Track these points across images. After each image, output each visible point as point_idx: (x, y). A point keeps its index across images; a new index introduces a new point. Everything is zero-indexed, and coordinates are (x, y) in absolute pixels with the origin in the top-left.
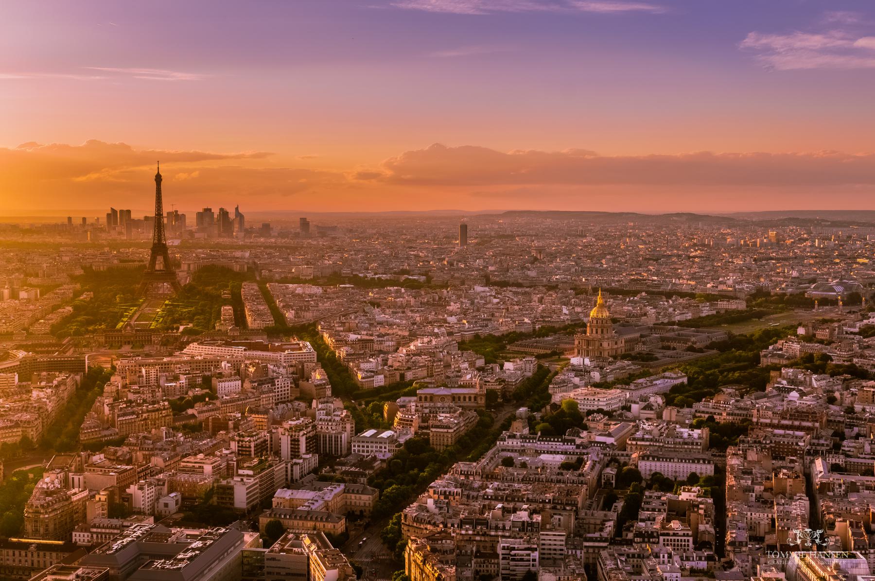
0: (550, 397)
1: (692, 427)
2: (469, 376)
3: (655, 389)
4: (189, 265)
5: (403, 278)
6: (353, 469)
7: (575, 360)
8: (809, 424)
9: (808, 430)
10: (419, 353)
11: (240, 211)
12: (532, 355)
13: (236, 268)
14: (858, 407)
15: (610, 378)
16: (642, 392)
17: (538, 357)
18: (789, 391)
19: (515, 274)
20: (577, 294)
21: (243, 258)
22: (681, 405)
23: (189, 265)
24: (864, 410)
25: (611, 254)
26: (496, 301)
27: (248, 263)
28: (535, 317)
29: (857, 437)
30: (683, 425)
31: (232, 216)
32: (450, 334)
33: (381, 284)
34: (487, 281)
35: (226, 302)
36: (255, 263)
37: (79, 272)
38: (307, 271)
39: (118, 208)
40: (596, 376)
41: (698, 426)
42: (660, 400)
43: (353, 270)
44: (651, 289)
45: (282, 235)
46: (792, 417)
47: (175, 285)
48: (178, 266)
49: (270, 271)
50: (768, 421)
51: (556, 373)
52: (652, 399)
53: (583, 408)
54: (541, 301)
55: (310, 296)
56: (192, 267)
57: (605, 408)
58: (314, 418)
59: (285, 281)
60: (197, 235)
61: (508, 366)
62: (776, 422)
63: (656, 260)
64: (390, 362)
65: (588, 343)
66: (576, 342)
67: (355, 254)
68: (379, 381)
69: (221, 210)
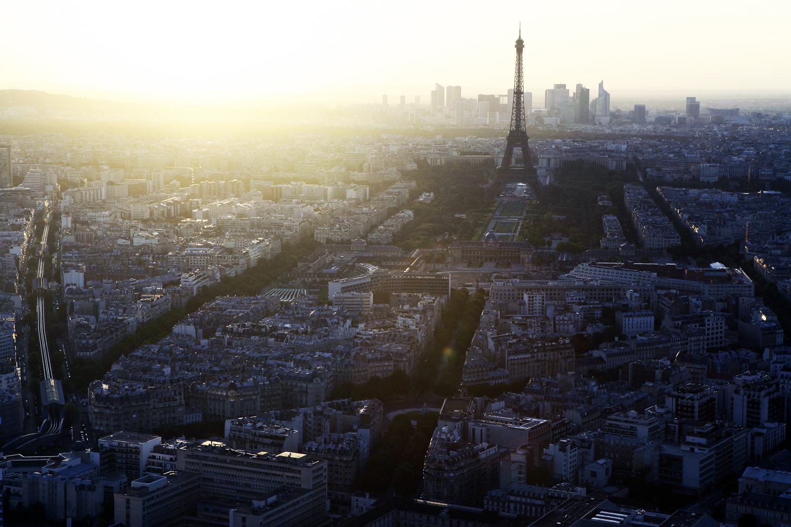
4: (549, 159)
11: (605, 88)
13: (612, 165)
21: (618, 151)
27: (626, 159)
31: (594, 95)
35: (605, 210)
36: (635, 158)
37: (412, 166)
39: (445, 84)
43: (775, 171)
47: (534, 185)
48: (536, 161)
49: (659, 170)
55: (723, 205)
56: (552, 162)
67: (776, 148)
69: (579, 86)
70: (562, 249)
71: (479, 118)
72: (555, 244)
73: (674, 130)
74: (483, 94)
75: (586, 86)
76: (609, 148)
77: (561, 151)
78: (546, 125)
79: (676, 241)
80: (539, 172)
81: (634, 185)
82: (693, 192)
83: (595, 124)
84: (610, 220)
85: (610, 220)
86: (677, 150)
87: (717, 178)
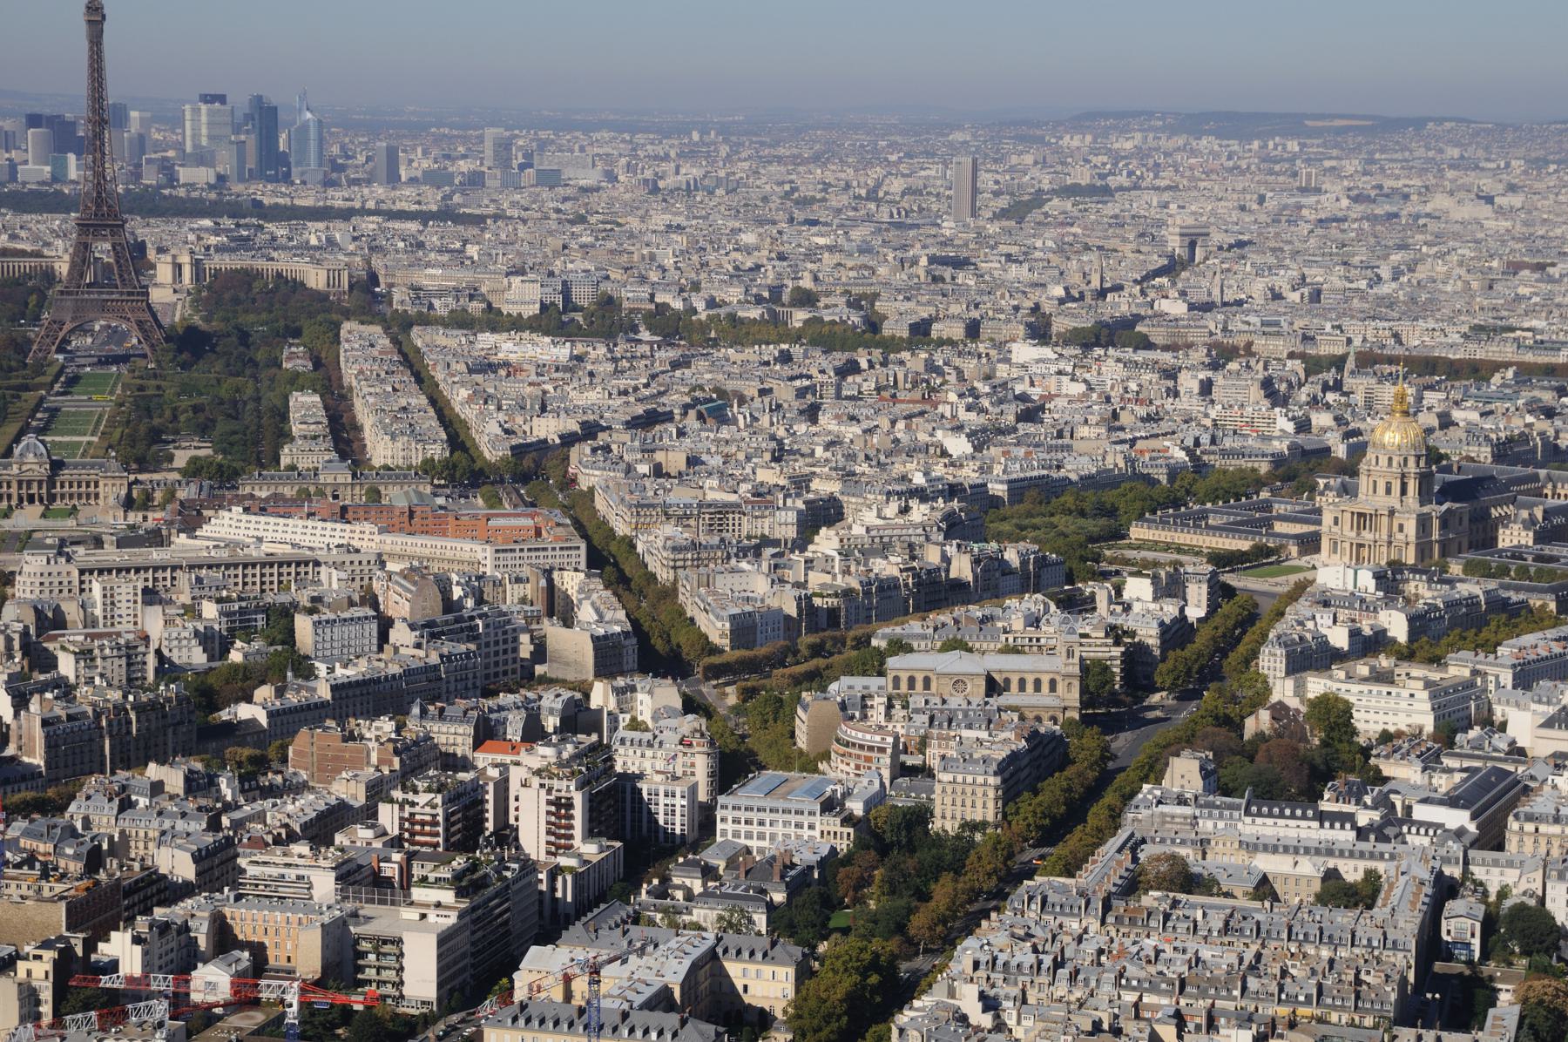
5: (799, 317)
13: (316, 279)
19: (1120, 306)
20: (1308, 373)
23: (180, 266)
25: (1403, 247)
26: (1078, 388)
28: (1197, 443)
33: (737, 331)
34: (1039, 332)
35: (296, 381)
38: (523, 297)
44: (1529, 357)
45: (434, 178)
54: (1206, 388)
55: (541, 369)
59: (461, 321)
60: (184, 174)
63: (1541, 267)
65: (1363, 520)
66: (1327, 518)
70: (194, 470)
71: (30, 166)
72: (181, 458)
73: (457, 198)
74: (37, 110)
75: (273, 98)
76: (314, 241)
77: (208, 248)
78: (184, 185)
79: (438, 451)
80: (159, 296)
81: (362, 323)
82: (486, 339)
83: (292, 183)
84: (305, 406)
85: (305, 406)
86: (458, 245)
87: (538, 306)
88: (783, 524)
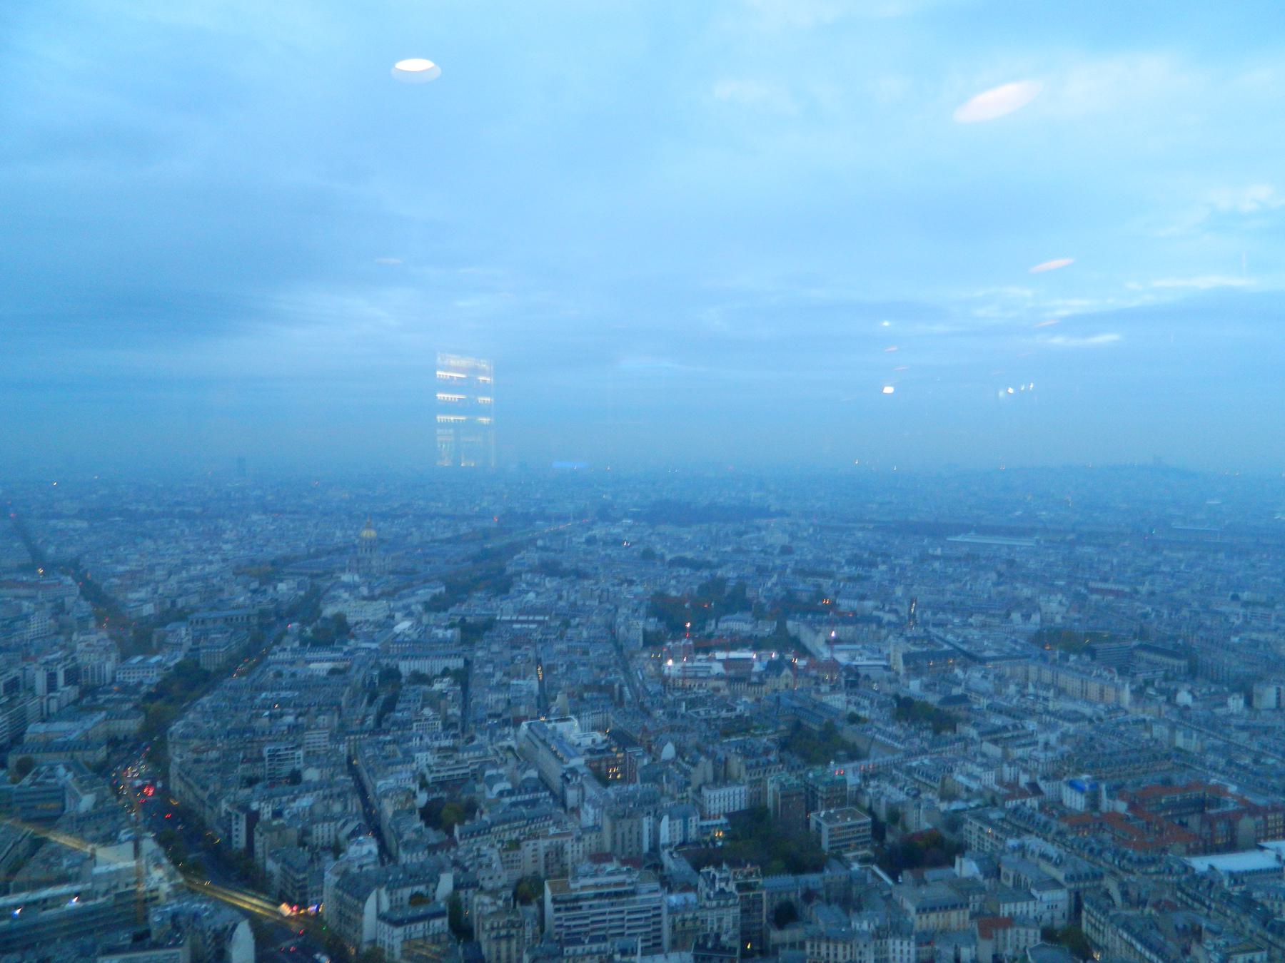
0: (321, 612)
1: (446, 628)
2: (242, 599)
3: (417, 598)
6: (117, 696)
7: (346, 578)
8: (541, 618)
9: (540, 623)
10: (191, 580)
12: (306, 574)
14: (580, 603)
15: (377, 592)
16: (405, 602)
17: (313, 576)
18: (528, 592)
22: (438, 610)
24: (584, 605)
29: (578, 625)
30: (438, 627)
32: (224, 560)
40: (364, 591)
41: (452, 626)
42: (420, 608)
46: (528, 614)
50: (508, 618)
51: (327, 591)
52: (413, 607)
53: (351, 619)
57: (371, 619)
58: (73, 651)
61: (282, 587)
62: (514, 618)
64: (160, 591)
65: (358, 561)
68: (148, 609)
88: (160, 573)
